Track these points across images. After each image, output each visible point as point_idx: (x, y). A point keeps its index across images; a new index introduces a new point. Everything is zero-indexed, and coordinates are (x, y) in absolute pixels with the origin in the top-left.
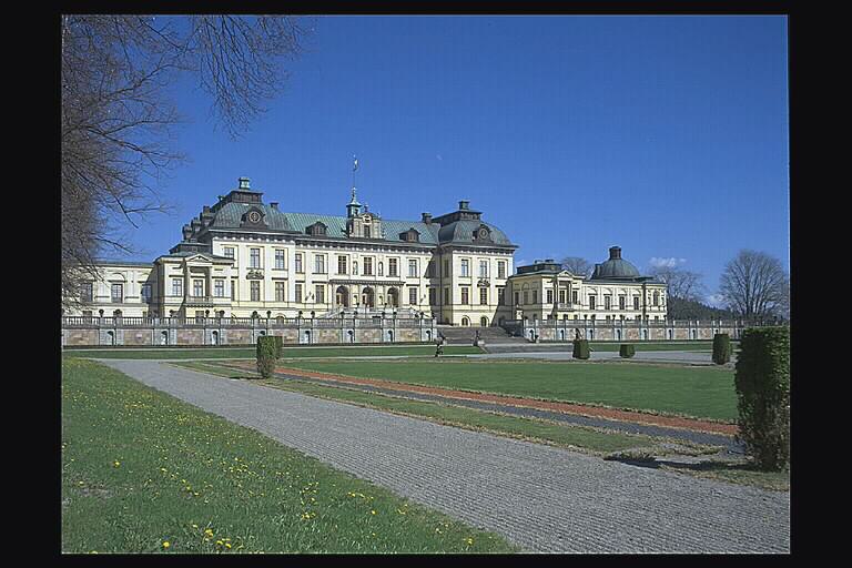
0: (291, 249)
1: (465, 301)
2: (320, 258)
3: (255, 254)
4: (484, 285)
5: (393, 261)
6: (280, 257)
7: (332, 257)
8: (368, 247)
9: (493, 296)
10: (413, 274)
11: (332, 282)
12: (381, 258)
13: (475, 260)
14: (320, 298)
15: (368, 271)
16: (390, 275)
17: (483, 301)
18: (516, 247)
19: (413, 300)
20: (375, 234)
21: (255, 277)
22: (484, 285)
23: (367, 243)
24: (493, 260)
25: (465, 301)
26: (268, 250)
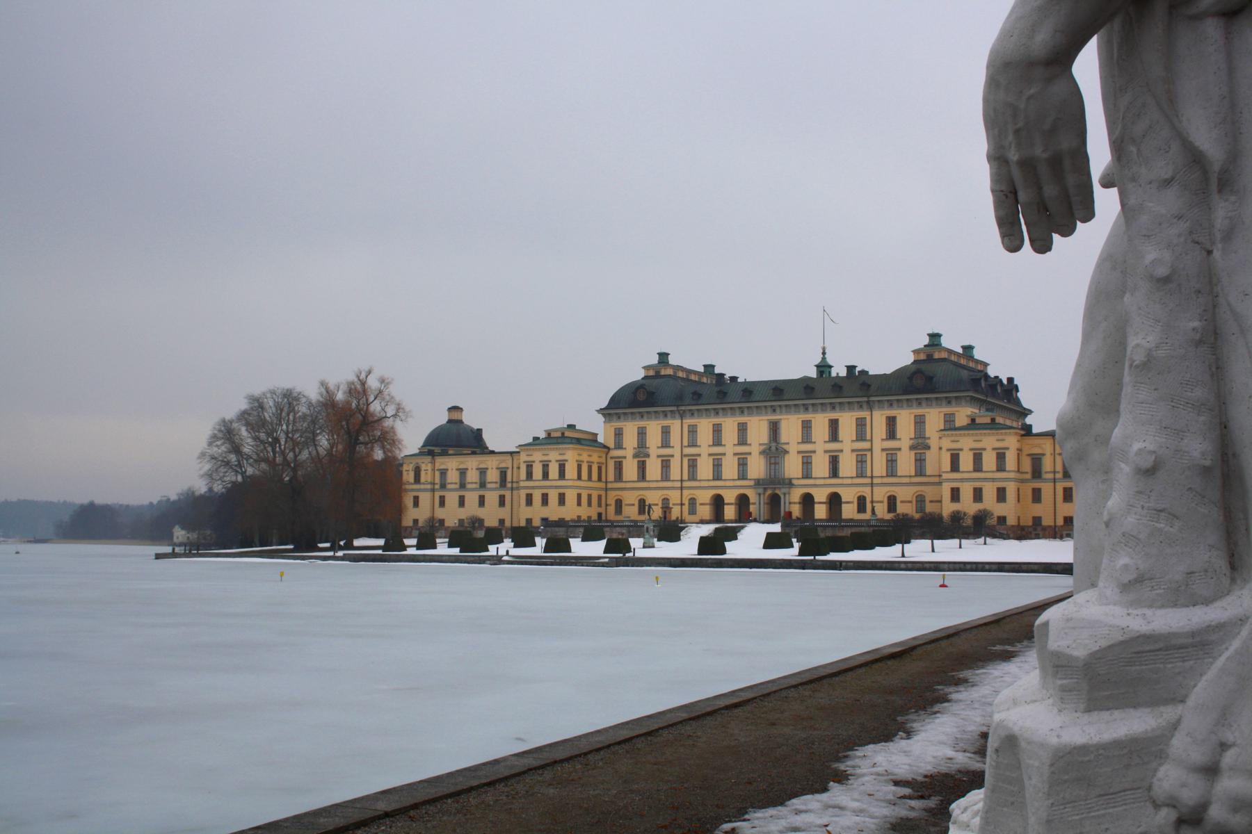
0: (675, 425)
3: (642, 433)
13: (905, 418)
21: (641, 453)
22: (920, 445)
26: (654, 428)
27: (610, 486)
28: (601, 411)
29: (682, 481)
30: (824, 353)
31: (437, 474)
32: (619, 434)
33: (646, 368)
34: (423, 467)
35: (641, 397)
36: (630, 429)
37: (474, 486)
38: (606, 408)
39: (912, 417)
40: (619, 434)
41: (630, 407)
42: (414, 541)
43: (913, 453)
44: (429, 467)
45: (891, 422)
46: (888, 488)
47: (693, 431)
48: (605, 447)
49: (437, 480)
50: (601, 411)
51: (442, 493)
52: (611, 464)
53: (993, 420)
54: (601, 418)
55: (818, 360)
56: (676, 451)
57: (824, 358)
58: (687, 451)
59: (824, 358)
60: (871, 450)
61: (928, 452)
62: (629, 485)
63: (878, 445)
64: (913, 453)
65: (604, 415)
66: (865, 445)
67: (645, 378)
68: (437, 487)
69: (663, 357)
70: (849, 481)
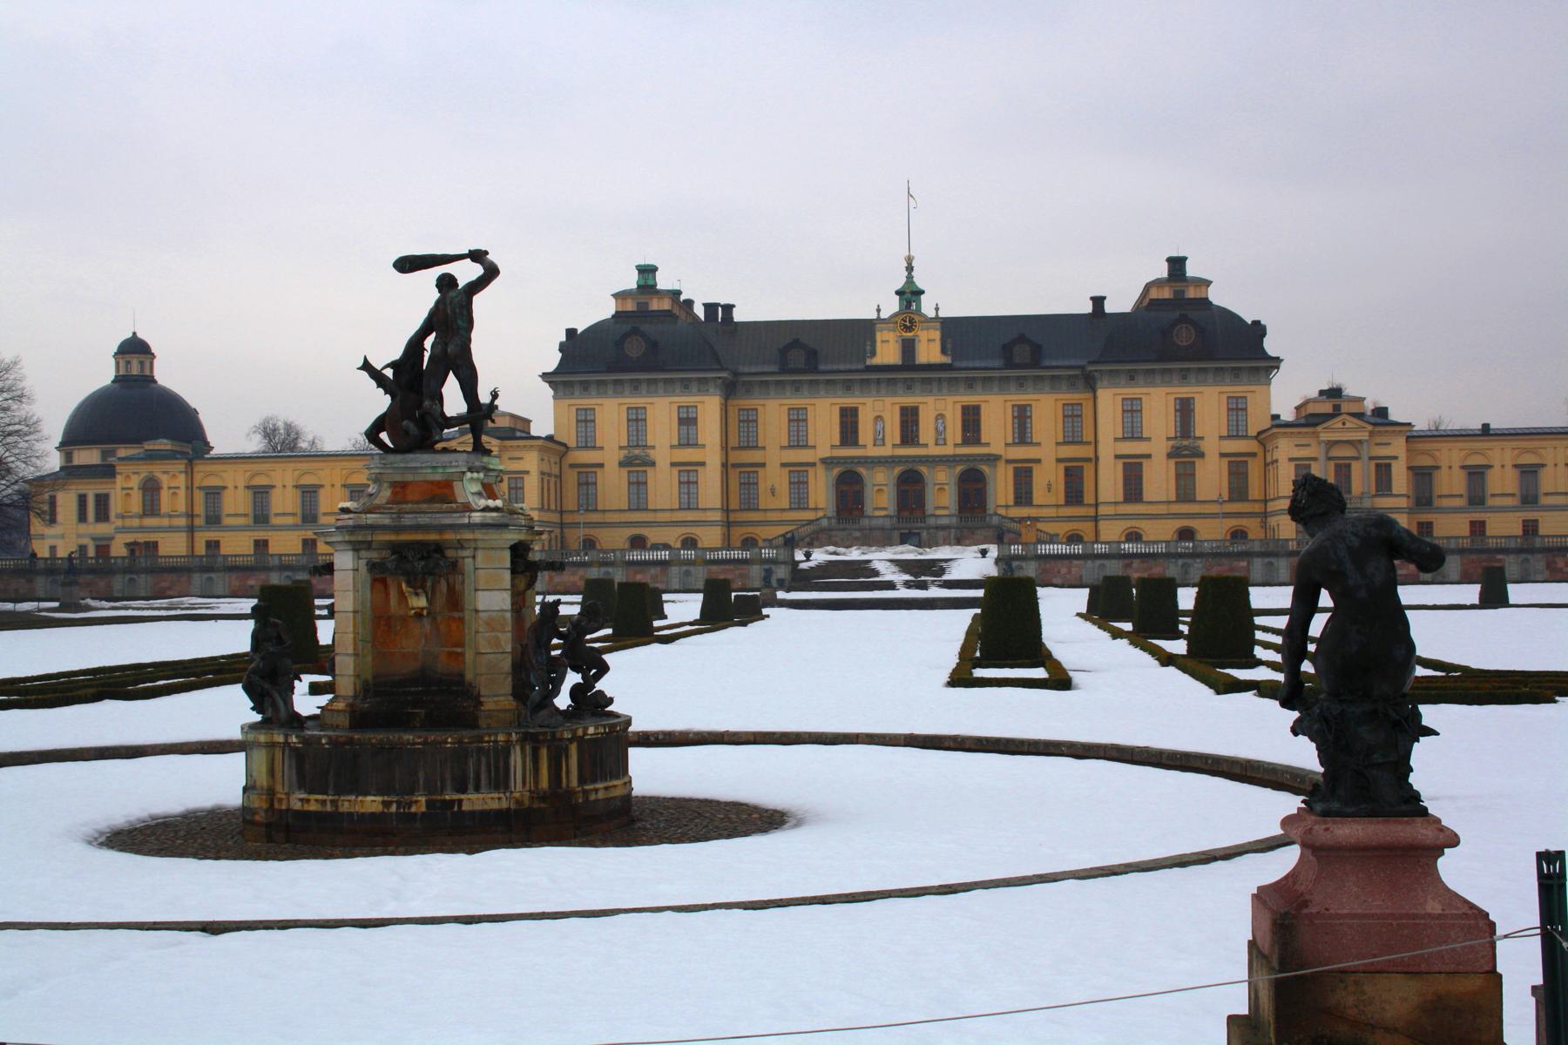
0: (709, 408)
1: (1133, 488)
2: (798, 419)
3: (637, 420)
4: (1185, 453)
5: (971, 421)
6: (687, 421)
7: (824, 413)
8: (909, 386)
9: (1211, 477)
10: (1022, 435)
11: (824, 461)
12: (940, 412)
13: (1158, 403)
14: (799, 503)
15: (909, 434)
16: (966, 441)
17: (1185, 489)
18: (1275, 362)
19: (1023, 495)
20: (929, 351)
21: (637, 462)
22: (1185, 453)
23: (909, 372)
24: (1210, 402)
25: (1133, 488)
26: (662, 411)
27: (568, 518)
28: (545, 376)
29: (726, 510)
30: (910, 268)
31: (199, 497)
32: (586, 420)
33: (620, 296)
34: (165, 480)
35: (634, 349)
36: (611, 412)
37: (289, 520)
38: (558, 371)
39: (1172, 403)
40: (586, 420)
41: (610, 370)
42: (564, 610)
43: (1172, 462)
44: (181, 480)
45: (1132, 410)
46: (1129, 524)
47: (750, 420)
48: (565, 445)
49: (200, 509)
50: (545, 376)
51: (213, 535)
52: (571, 478)
53: (1337, 408)
54: (548, 391)
55: (900, 282)
56: (712, 457)
57: (910, 278)
58: (735, 457)
59: (910, 278)
60: (1097, 458)
61: (1198, 462)
62: (610, 518)
63: (1107, 449)
64: (1172, 462)
65: (550, 383)
66: (1086, 451)
67: (618, 315)
68: (199, 522)
69: (647, 271)
70: (1215, 509)
